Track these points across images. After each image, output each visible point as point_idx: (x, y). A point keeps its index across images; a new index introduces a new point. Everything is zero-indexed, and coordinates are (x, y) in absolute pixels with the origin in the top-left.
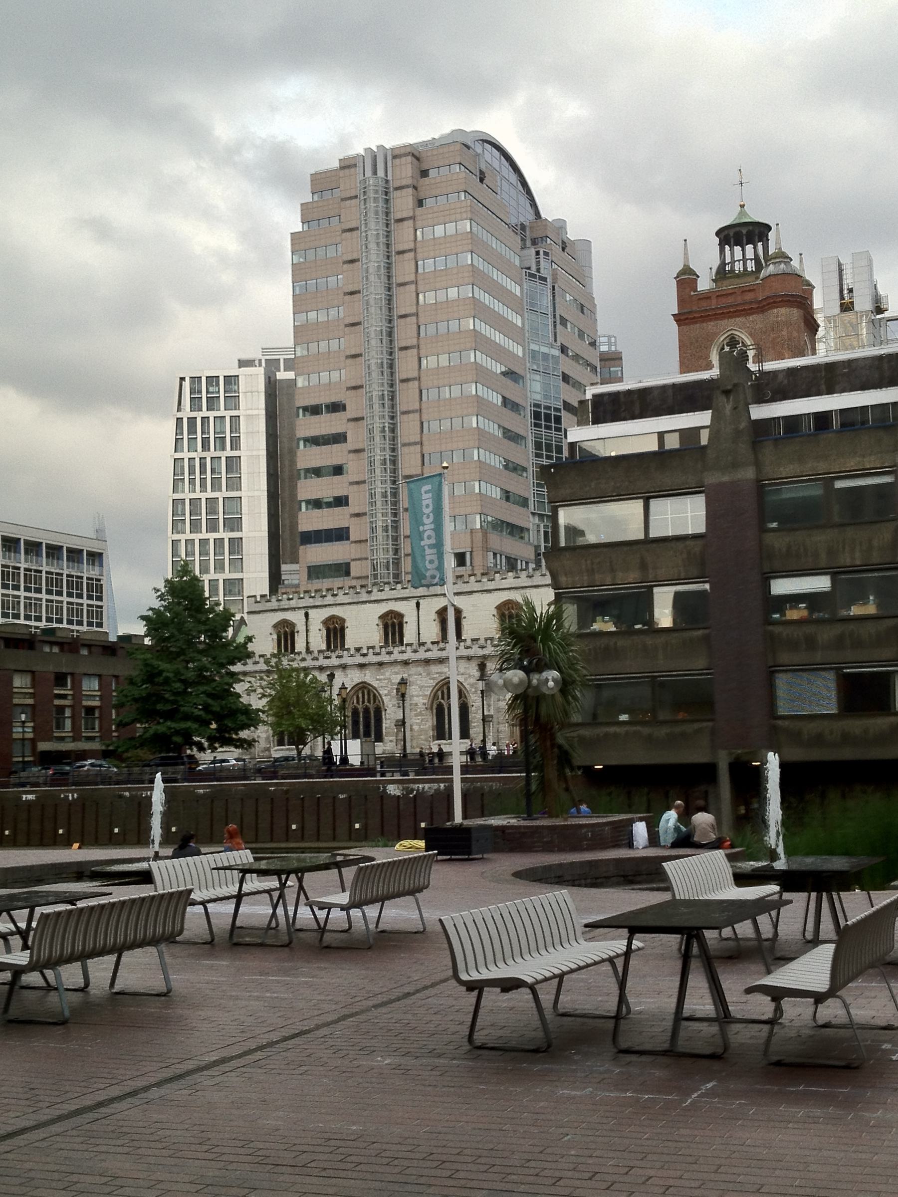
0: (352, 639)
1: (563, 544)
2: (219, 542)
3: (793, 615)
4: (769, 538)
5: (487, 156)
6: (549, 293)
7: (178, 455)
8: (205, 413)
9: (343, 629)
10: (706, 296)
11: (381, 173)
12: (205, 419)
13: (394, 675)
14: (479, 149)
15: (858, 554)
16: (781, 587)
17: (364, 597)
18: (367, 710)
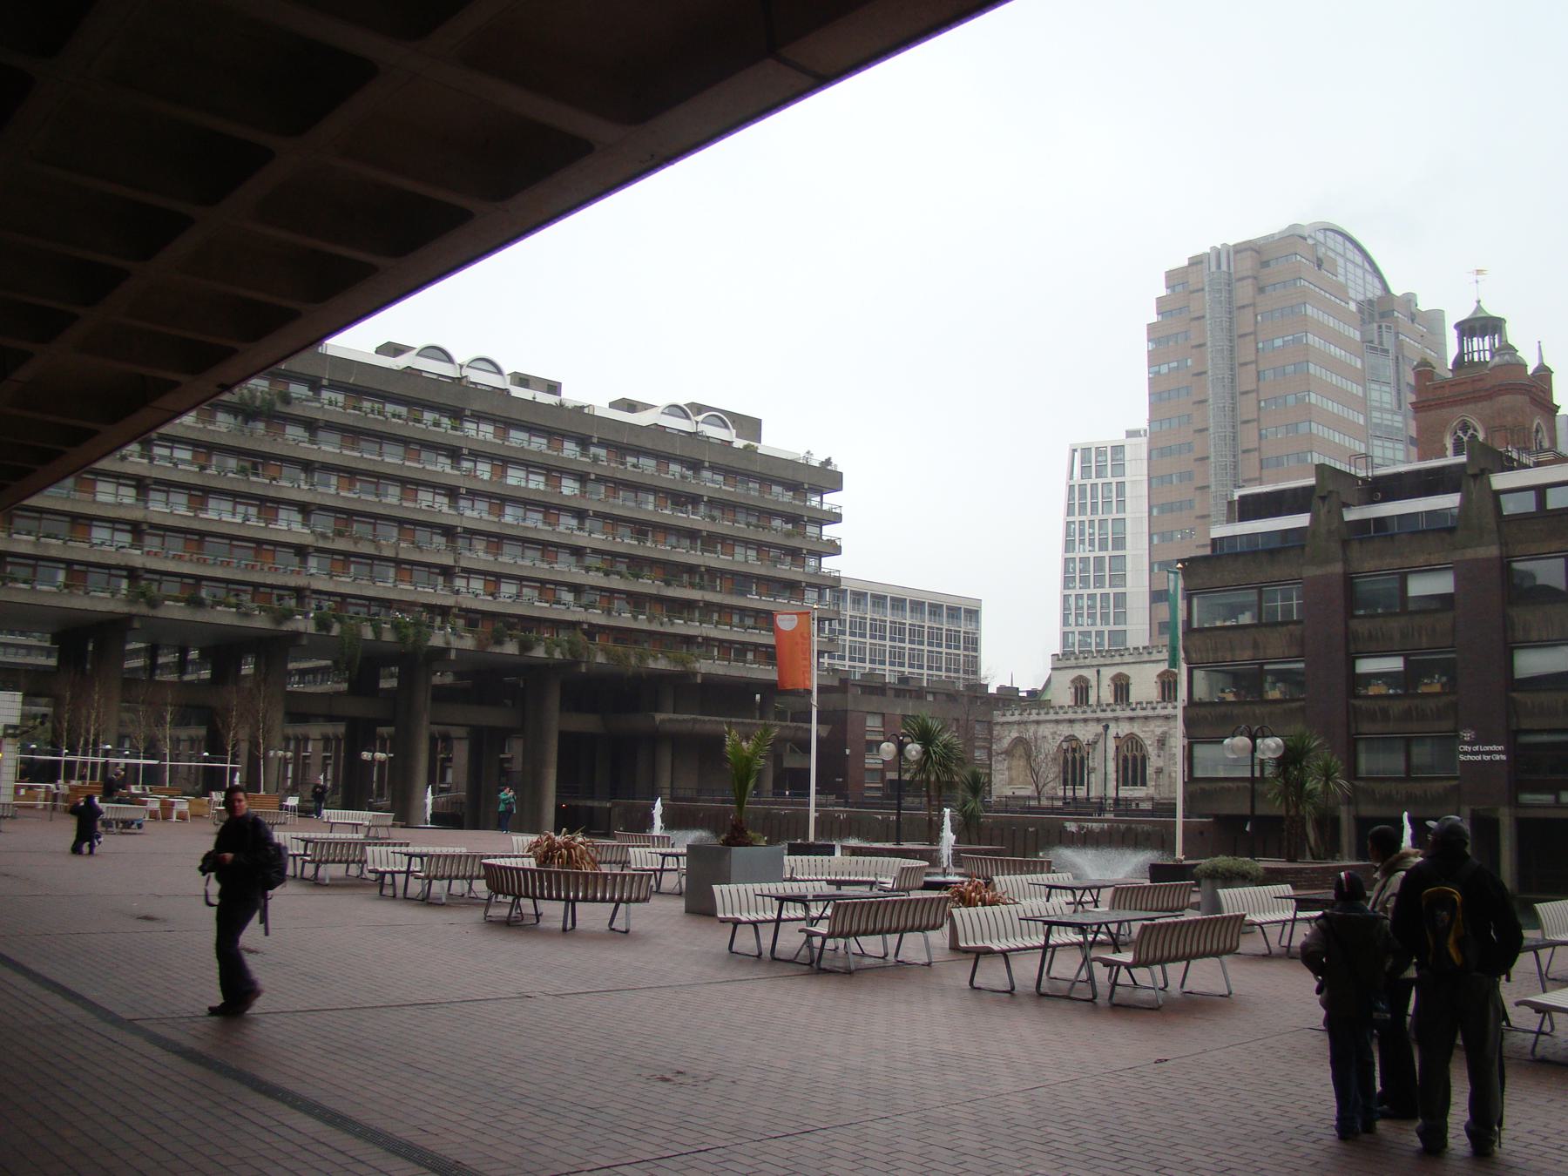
0: (1135, 695)
1: (1195, 625)
2: (1105, 596)
3: (1372, 691)
4: (1354, 623)
5: (1331, 244)
6: (1391, 363)
7: (1071, 519)
8: (1094, 480)
9: (1128, 685)
10: (1445, 384)
11: (1224, 267)
12: (1094, 486)
13: (1158, 729)
14: (1320, 237)
15: (1424, 639)
16: (1365, 666)
17: (1146, 657)
18: (1135, 758)
